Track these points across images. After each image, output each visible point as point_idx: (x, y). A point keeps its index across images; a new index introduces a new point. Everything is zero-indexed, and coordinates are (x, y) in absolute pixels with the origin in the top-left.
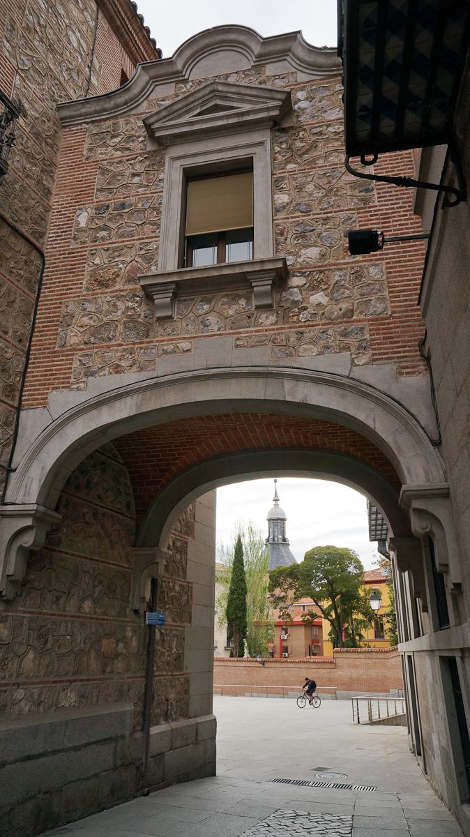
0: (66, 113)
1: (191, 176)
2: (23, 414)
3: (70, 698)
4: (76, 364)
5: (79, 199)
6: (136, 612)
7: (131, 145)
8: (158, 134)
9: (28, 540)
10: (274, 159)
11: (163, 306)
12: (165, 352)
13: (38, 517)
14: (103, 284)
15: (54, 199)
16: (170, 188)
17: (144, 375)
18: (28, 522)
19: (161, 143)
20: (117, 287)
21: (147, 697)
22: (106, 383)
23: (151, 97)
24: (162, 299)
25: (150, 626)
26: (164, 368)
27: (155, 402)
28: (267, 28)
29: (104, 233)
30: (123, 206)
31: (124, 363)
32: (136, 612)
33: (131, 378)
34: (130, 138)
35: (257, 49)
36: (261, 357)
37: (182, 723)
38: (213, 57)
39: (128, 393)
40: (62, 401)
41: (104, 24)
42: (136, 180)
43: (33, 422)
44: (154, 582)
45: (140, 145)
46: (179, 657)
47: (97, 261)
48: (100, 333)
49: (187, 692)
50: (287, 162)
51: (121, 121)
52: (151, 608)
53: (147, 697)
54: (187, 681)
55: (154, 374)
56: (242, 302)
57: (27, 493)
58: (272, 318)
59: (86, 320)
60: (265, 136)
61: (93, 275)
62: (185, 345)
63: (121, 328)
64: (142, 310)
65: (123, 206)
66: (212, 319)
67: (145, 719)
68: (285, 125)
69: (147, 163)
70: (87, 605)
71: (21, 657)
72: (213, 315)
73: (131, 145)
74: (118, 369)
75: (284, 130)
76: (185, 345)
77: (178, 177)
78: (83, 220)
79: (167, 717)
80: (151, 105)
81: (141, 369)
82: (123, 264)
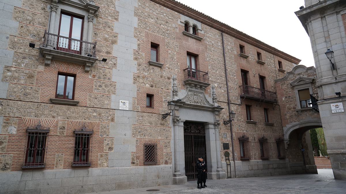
0: (276, 81)
1: (299, 91)
2: (283, 128)
3: (295, 161)
4: (289, 121)
5: (282, 95)
6: (300, 149)
7: (288, 86)
8: (293, 85)
9: (288, 143)
10: (312, 88)
11: (300, 113)
12: (302, 119)
13: (289, 140)
14: (290, 109)
15: (278, 96)
16: (297, 94)
17: (299, 122)
18: (288, 141)
19: (293, 87)
20: (292, 110)
21: (304, 161)
22: (294, 123)
23: (289, 77)
24: (299, 112)
25: (303, 151)
26: (301, 121)
27: (301, 126)
28: (308, 66)
29: (288, 101)
30: (289, 97)
31: (296, 121)
32: (300, 149)
33: (297, 123)
34: (287, 85)
35: (306, 69)
36: (315, 119)
37: (310, 165)
38: (298, 69)
39: (298, 125)
40: (288, 126)
41: (275, 56)
42: (290, 92)
43: (285, 129)
44: (302, 145)
45: (289, 86)
46: (308, 156)
47: (288, 106)
48: (291, 117)
49: (310, 161)
50: (315, 89)
51: (285, 81)
52: (302, 149)
53: (304, 161)
54: (310, 159)
55: (300, 122)
56: (311, 112)
57: (287, 138)
58: (316, 114)
59: (288, 115)
60: (310, 85)
61: (288, 108)
62: (304, 118)
63: (294, 116)
64: (297, 113)
65: (289, 97)
66: (307, 114)
67: (305, 164)
68: (314, 82)
69: (291, 89)
70: (294, 149)
71: (290, 156)
72: (308, 114)
73: (288, 86)
74: (295, 122)
75: (313, 83)
76: (304, 118)
77: (297, 92)
78: (283, 99)
79: (308, 164)
80: (289, 79)
81: (299, 121)
82: (292, 106)
